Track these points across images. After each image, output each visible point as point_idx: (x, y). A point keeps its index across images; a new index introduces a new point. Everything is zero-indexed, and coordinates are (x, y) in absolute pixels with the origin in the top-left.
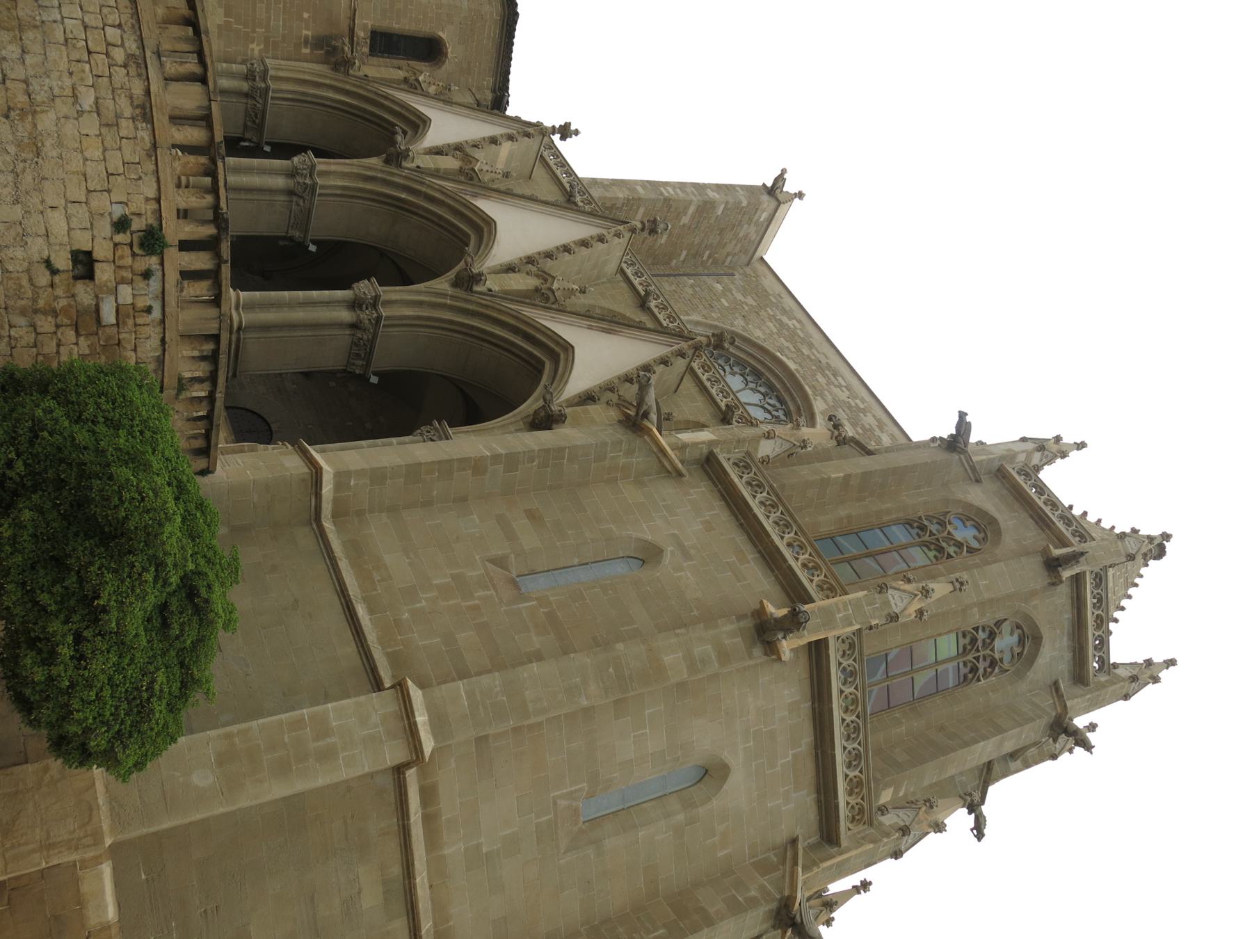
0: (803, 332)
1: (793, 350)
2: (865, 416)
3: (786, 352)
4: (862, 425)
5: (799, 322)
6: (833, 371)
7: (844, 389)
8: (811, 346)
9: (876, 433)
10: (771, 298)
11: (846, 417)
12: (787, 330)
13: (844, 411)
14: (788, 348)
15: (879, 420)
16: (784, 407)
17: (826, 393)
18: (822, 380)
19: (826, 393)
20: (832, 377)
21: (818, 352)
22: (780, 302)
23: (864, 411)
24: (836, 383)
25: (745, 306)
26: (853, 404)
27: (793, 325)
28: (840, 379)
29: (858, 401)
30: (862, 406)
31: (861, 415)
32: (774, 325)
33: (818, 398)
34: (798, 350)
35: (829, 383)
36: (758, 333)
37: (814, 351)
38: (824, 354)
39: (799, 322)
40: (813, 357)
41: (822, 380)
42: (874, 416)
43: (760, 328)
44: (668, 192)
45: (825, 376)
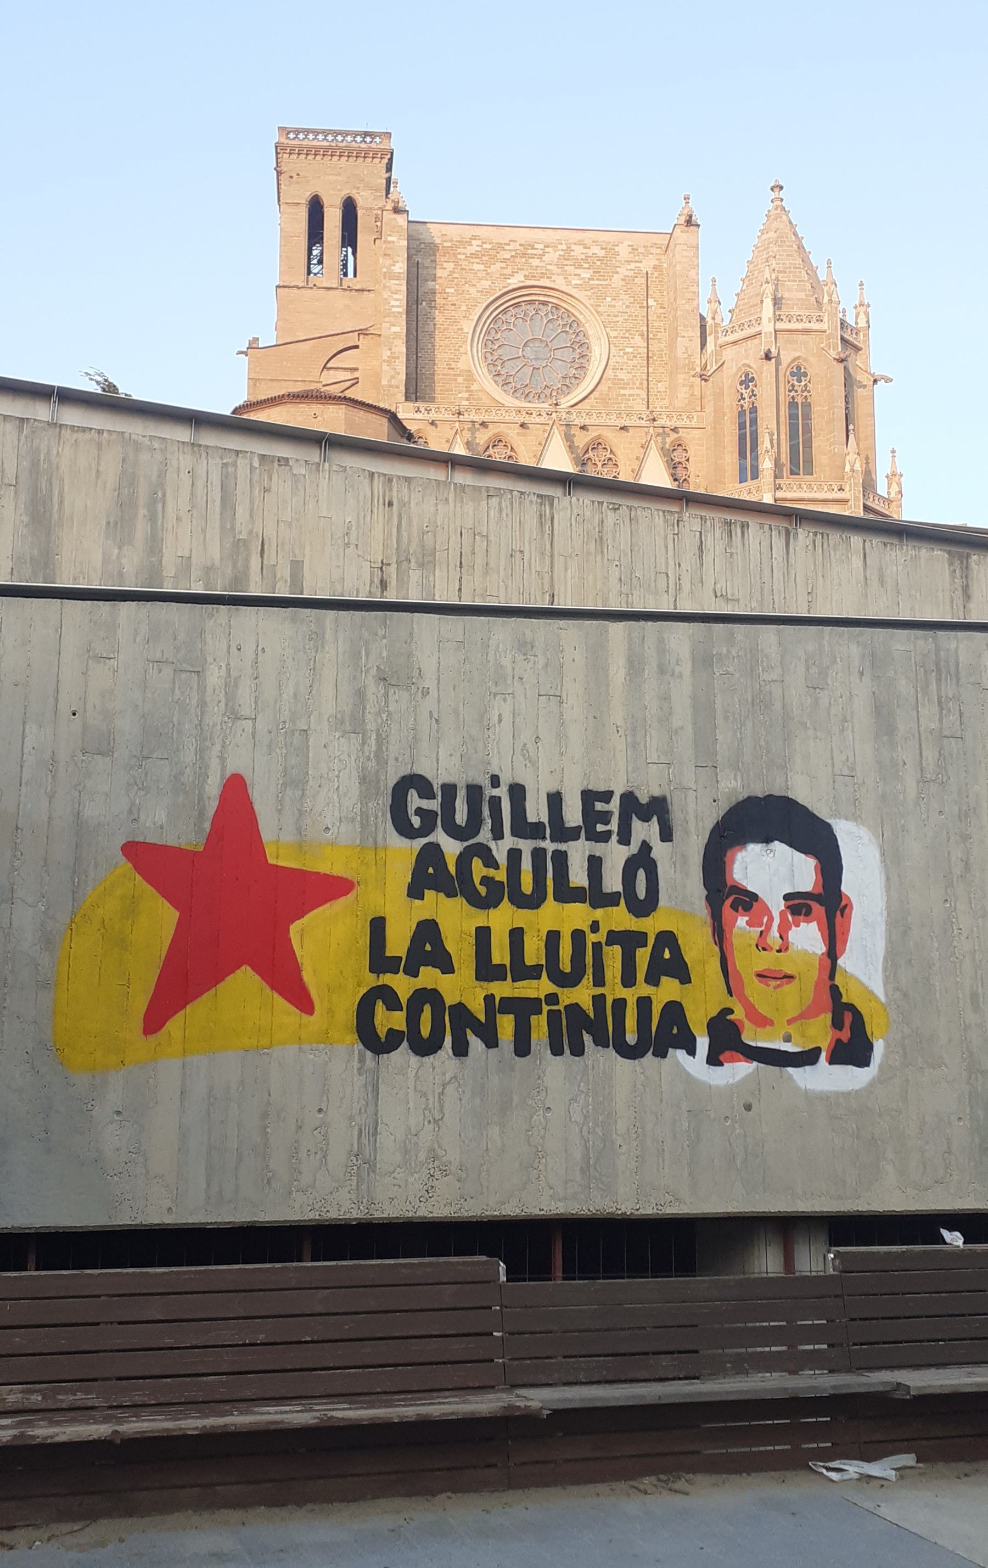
0: (486, 243)
1: (504, 265)
2: (573, 251)
3: (505, 271)
4: (582, 259)
5: (474, 238)
6: (529, 245)
7: (547, 250)
8: (500, 247)
9: (590, 254)
10: (446, 244)
11: (573, 267)
12: (484, 255)
13: (567, 265)
14: (501, 268)
15: (580, 243)
16: (550, 305)
17: (549, 267)
18: (535, 262)
19: (549, 267)
20: (534, 252)
21: (509, 245)
22: (451, 241)
23: (569, 250)
24: (541, 252)
25: (455, 275)
26: (562, 253)
27: (477, 246)
28: (536, 246)
29: (560, 247)
30: (564, 247)
31: (572, 253)
32: (477, 263)
33: (554, 278)
34: (505, 260)
35: (540, 257)
36: (486, 284)
37: (506, 247)
38: (510, 241)
39: (474, 238)
40: (513, 253)
41: (535, 262)
42: (575, 244)
43: (480, 279)
44: (398, 306)
45: (533, 256)
